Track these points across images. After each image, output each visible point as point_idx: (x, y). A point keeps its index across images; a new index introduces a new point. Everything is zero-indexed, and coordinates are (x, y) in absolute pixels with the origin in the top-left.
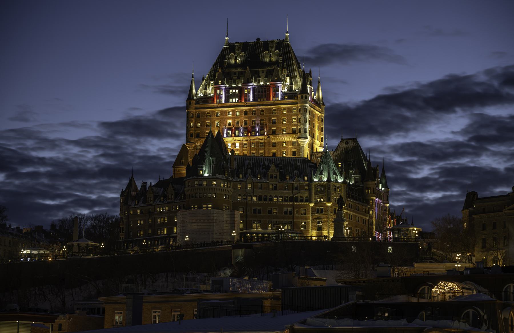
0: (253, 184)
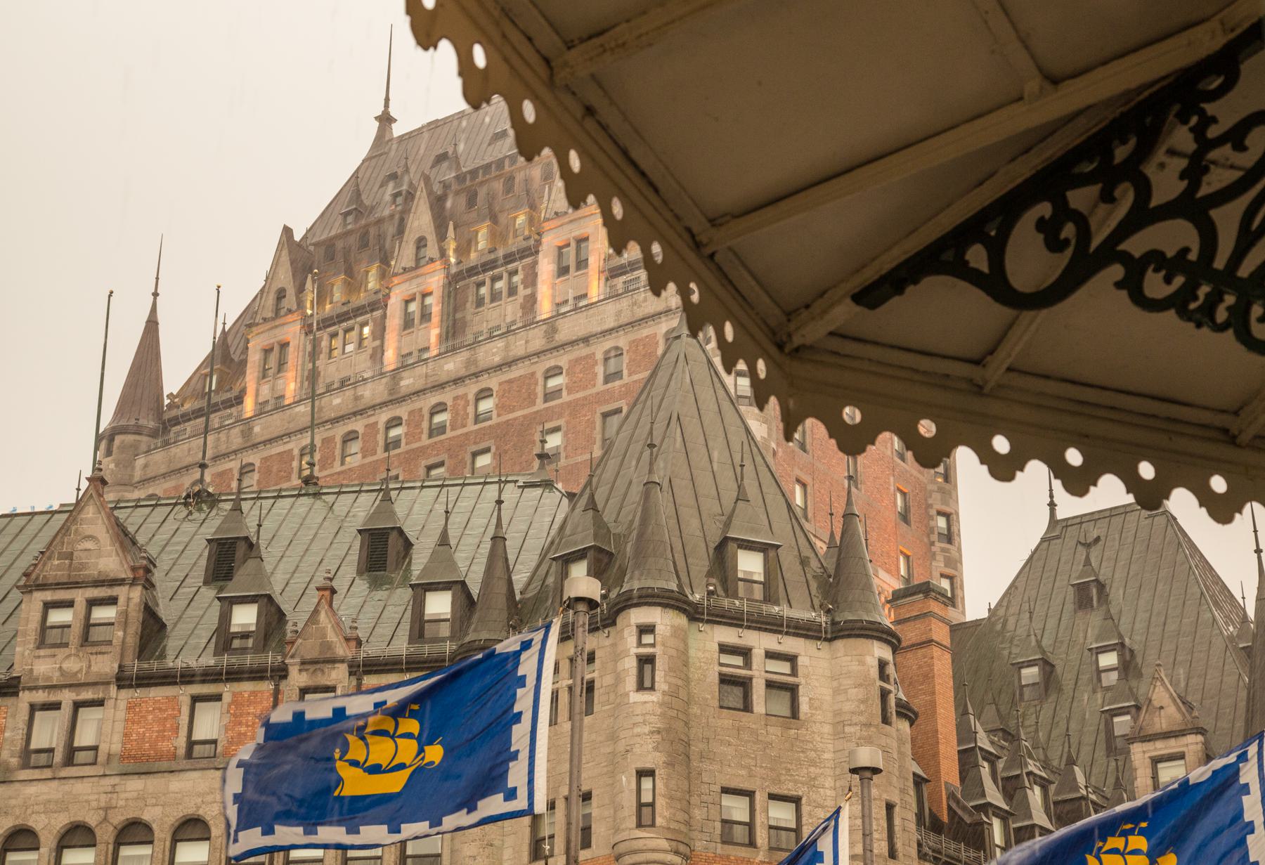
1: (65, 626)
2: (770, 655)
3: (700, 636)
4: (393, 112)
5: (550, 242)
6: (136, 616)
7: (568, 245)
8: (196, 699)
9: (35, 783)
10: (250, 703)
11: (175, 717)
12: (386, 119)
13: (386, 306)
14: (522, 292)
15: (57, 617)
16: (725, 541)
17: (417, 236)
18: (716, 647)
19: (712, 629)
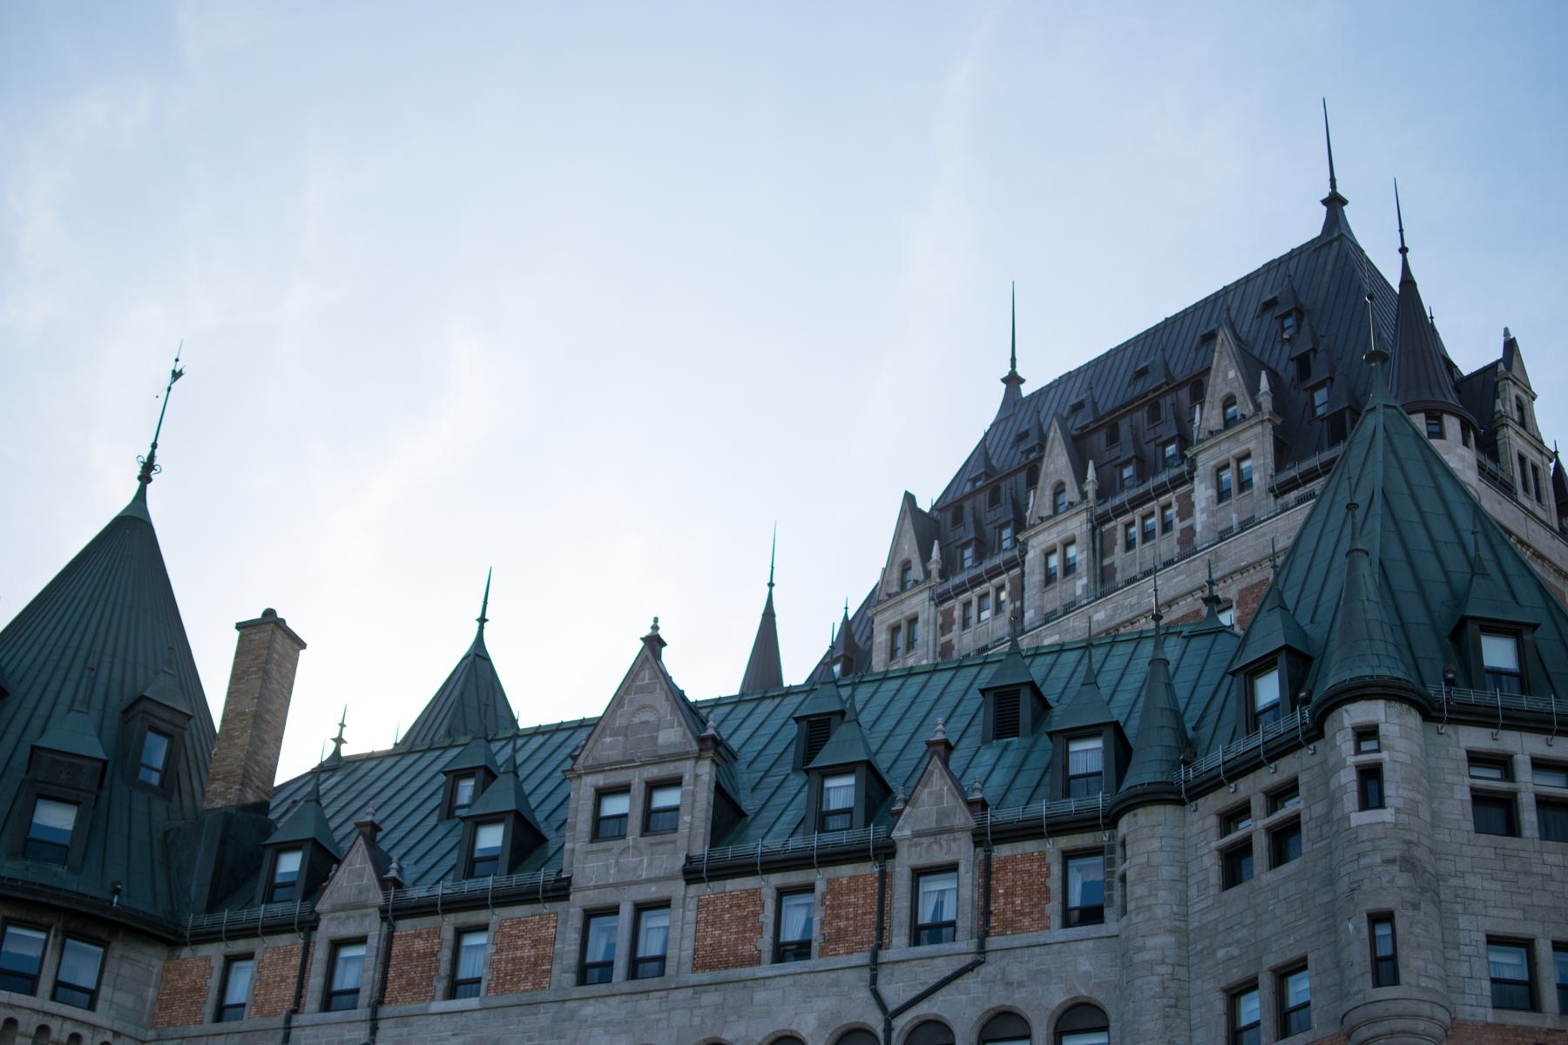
0: (390, 939)
1: (623, 817)
2: (1539, 764)
3: (1440, 739)
4: (1020, 372)
5: (1206, 462)
6: (705, 797)
7: (1226, 466)
8: (782, 893)
9: (592, 1002)
10: (850, 891)
11: (755, 914)
12: (1013, 380)
13: (1024, 562)
14: (1178, 525)
15: (615, 806)
16: (1464, 621)
17: (1053, 481)
18: (1463, 754)
19: (1456, 732)
